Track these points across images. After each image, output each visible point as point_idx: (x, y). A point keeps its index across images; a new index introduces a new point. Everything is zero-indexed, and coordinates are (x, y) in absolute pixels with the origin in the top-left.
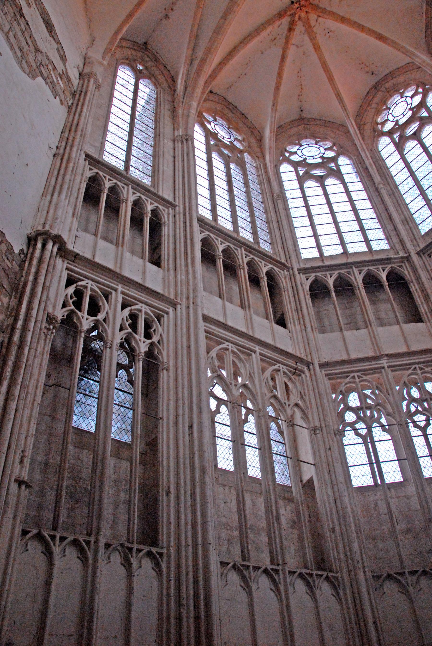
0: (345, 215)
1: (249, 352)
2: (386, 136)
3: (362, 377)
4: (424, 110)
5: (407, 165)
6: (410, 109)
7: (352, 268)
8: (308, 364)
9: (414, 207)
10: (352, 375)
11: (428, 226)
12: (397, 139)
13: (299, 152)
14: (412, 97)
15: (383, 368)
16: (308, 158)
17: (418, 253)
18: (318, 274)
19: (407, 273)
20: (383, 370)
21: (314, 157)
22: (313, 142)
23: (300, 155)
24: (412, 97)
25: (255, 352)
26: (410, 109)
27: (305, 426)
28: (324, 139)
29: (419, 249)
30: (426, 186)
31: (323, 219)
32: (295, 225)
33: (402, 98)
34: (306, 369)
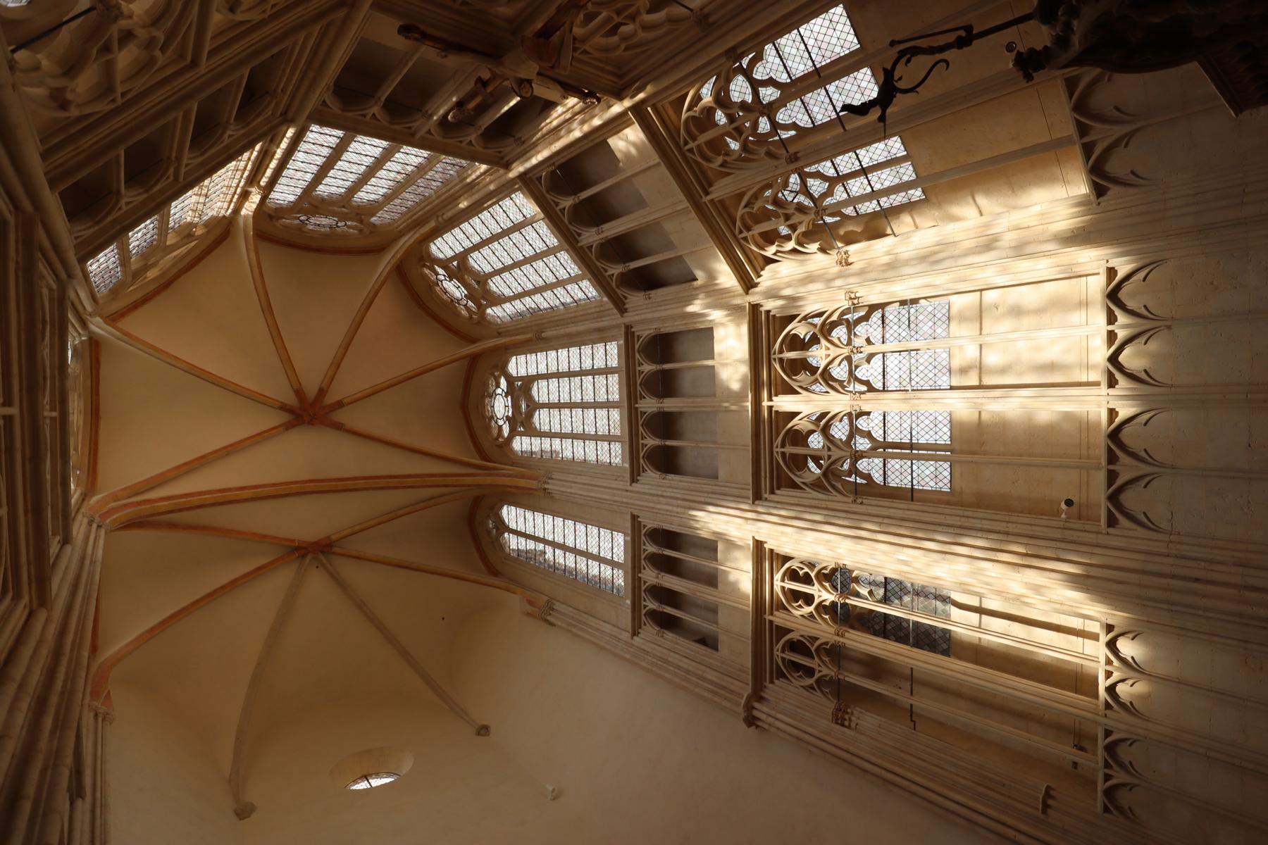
14: (498, 386)
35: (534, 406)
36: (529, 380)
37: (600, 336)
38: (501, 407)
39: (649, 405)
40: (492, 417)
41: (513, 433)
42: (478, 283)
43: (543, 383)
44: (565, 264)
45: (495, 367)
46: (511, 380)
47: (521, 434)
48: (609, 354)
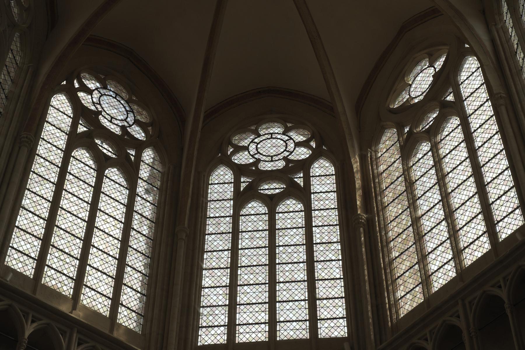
0: (106, 242)
4: (302, 175)
5: (236, 233)
6: (285, 159)
9: (209, 298)
12: (243, 186)
13: (96, 95)
14: (298, 144)
21: (114, 121)
26: (285, 159)
30: (243, 280)
32: (25, 202)
33: (284, 134)
35: (272, 203)
36: (304, 194)
38: (272, 146)
40: (259, 136)
41: (239, 171)
43: (300, 220)
46: (305, 166)
47: (237, 183)
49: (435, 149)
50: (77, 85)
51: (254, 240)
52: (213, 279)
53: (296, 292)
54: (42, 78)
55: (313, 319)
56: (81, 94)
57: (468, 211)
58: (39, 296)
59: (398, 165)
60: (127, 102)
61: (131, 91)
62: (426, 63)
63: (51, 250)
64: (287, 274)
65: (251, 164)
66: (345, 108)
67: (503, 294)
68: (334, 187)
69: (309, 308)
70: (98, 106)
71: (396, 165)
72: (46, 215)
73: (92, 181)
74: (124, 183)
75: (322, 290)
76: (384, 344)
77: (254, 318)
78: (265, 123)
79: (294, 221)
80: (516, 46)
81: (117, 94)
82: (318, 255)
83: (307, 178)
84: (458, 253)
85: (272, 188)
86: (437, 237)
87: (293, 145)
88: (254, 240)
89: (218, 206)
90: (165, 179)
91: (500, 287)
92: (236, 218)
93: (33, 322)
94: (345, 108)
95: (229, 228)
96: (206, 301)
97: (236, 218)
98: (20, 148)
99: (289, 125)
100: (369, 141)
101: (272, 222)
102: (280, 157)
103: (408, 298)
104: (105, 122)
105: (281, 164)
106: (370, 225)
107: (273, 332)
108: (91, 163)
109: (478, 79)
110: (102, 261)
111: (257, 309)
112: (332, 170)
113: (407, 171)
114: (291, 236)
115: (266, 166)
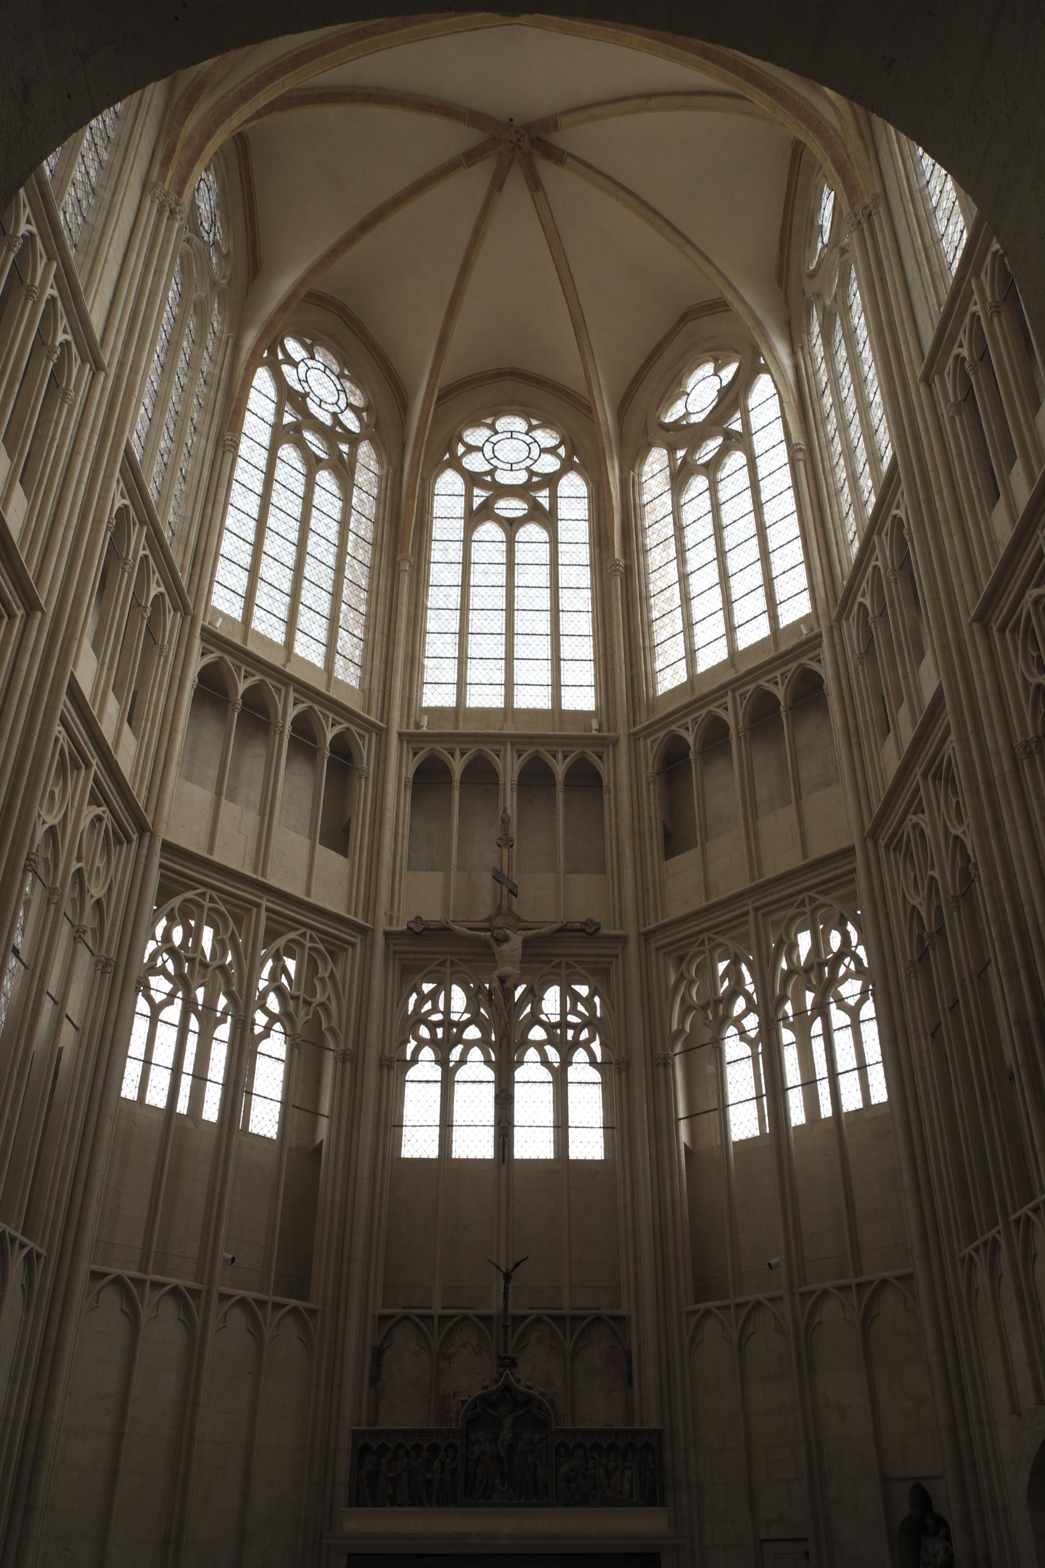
1: (76, 761)
2: (463, 477)
3: (217, 903)
5: (466, 564)
7: (287, 686)
8: (143, 829)
10: (202, 890)
11: (439, 698)
12: (477, 502)
13: (302, 368)
14: (543, 451)
15: (258, 906)
16: (311, 395)
17: (401, 735)
18: (228, 659)
19: (366, 752)
20: (255, 910)
22: (336, 368)
23: (302, 377)
24: (543, 451)
25: (88, 766)
26: (527, 469)
27: (90, 944)
28: (358, 380)
29: (404, 730)
31: (279, 547)
33: (527, 434)
34: (135, 837)
35: (511, 526)
36: (548, 518)
37: (605, 682)
38: (511, 446)
39: (509, 768)
40: (496, 433)
41: (472, 479)
42: (706, 465)
43: (543, 553)
44: (712, 655)
45: (572, 451)
46: (551, 481)
47: (469, 497)
48: (581, 697)
49: (713, 489)
50: (280, 356)
51: (488, 575)
52: (440, 622)
53: (537, 648)
54: (245, 354)
55: (557, 685)
56: (286, 369)
57: (747, 580)
58: (250, 647)
59: (667, 499)
60: (338, 377)
61: (343, 362)
62: (709, 368)
63: (261, 585)
64: (527, 624)
65: (486, 473)
66: (606, 413)
67: (780, 693)
68: (585, 515)
69: (552, 671)
70: (305, 385)
71: (663, 498)
72: (251, 538)
73: (300, 490)
74: (336, 492)
75: (567, 648)
76: (638, 727)
77: (487, 677)
78: (504, 416)
79: (537, 555)
80: (824, 384)
81: (326, 367)
82: (563, 604)
83: (554, 498)
84: (731, 630)
85: (511, 507)
86: (707, 603)
87: (537, 451)
88: (488, 575)
89: (445, 526)
90: (383, 486)
91: (776, 683)
92: (467, 543)
93: (245, 677)
94: (606, 413)
95: (458, 557)
96: (431, 650)
97: (467, 543)
98: (224, 453)
99: (534, 422)
100: (632, 459)
101: (511, 553)
102: (523, 465)
103: (669, 675)
104: (313, 408)
105: (521, 478)
106: (628, 571)
107: (509, 696)
108: (299, 465)
109: (773, 409)
110: (316, 598)
111: (491, 666)
112: (583, 490)
113: (677, 510)
114: (533, 576)
115: (504, 478)
